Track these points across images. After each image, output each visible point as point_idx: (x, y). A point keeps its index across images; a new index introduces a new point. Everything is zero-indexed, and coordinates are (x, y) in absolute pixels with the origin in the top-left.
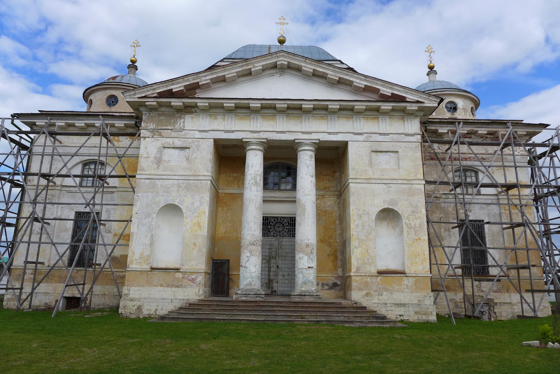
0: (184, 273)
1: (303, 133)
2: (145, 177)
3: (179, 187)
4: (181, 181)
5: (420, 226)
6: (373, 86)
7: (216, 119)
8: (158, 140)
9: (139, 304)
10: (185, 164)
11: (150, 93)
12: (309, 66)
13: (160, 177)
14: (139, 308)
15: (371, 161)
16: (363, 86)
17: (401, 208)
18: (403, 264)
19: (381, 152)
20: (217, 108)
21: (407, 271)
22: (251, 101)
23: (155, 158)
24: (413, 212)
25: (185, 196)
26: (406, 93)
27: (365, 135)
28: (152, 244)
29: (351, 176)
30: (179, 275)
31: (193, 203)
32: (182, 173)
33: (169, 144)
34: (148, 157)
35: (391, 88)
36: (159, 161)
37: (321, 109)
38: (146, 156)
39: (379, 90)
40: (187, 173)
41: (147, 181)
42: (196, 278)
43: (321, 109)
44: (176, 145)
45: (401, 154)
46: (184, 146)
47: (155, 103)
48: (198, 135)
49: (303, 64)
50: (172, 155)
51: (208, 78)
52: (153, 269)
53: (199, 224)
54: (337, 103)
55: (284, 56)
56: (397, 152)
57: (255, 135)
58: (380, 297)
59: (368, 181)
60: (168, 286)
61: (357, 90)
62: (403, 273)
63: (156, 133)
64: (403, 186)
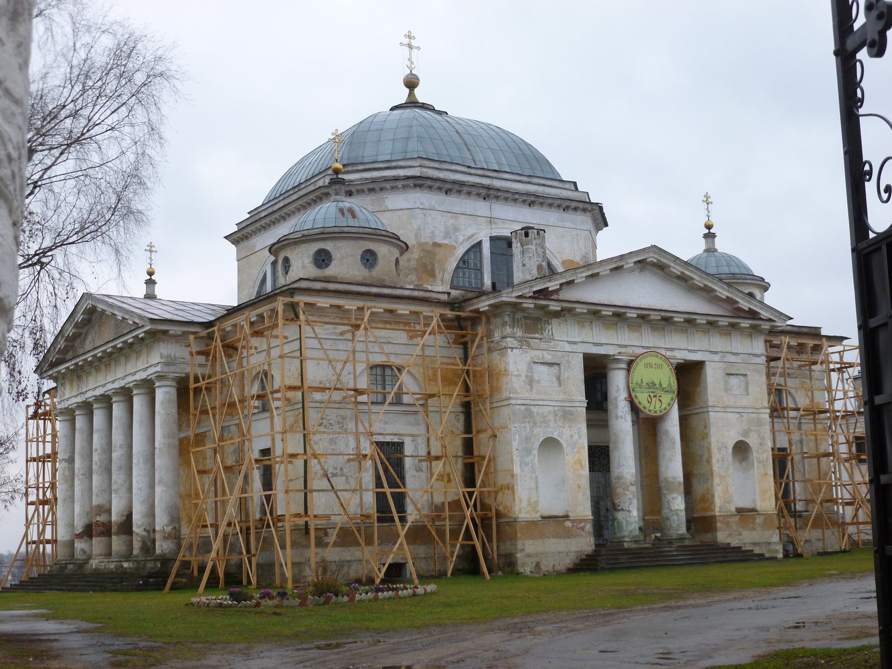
0: (573, 521)
2: (519, 402)
3: (556, 415)
4: (556, 408)
5: (767, 459)
6: (734, 298)
7: (583, 326)
8: (527, 352)
9: (537, 559)
10: (556, 384)
11: (526, 291)
12: (678, 267)
13: (536, 403)
14: (538, 565)
16: (724, 297)
18: (754, 501)
19: (732, 374)
20: (595, 314)
21: (758, 509)
22: (628, 310)
23: (526, 376)
24: (761, 444)
25: (563, 427)
26: (762, 309)
27: (721, 354)
28: (537, 488)
29: (710, 404)
31: (572, 436)
32: (556, 398)
33: (539, 358)
34: (519, 375)
36: (531, 381)
37: (690, 323)
38: (516, 373)
39: (737, 302)
40: (562, 397)
41: (523, 408)
42: (585, 526)
43: (690, 323)
44: (546, 360)
45: (750, 378)
46: (554, 361)
47: (532, 306)
48: (568, 348)
49: (672, 265)
50: (542, 372)
52: (543, 517)
54: (705, 317)
55: (654, 252)
56: (745, 375)
57: (623, 350)
58: (740, 537)
59: (725, 409)
61: (714, 299)
62: (754, 510)
63: (524, 343)
64: (753, 415)
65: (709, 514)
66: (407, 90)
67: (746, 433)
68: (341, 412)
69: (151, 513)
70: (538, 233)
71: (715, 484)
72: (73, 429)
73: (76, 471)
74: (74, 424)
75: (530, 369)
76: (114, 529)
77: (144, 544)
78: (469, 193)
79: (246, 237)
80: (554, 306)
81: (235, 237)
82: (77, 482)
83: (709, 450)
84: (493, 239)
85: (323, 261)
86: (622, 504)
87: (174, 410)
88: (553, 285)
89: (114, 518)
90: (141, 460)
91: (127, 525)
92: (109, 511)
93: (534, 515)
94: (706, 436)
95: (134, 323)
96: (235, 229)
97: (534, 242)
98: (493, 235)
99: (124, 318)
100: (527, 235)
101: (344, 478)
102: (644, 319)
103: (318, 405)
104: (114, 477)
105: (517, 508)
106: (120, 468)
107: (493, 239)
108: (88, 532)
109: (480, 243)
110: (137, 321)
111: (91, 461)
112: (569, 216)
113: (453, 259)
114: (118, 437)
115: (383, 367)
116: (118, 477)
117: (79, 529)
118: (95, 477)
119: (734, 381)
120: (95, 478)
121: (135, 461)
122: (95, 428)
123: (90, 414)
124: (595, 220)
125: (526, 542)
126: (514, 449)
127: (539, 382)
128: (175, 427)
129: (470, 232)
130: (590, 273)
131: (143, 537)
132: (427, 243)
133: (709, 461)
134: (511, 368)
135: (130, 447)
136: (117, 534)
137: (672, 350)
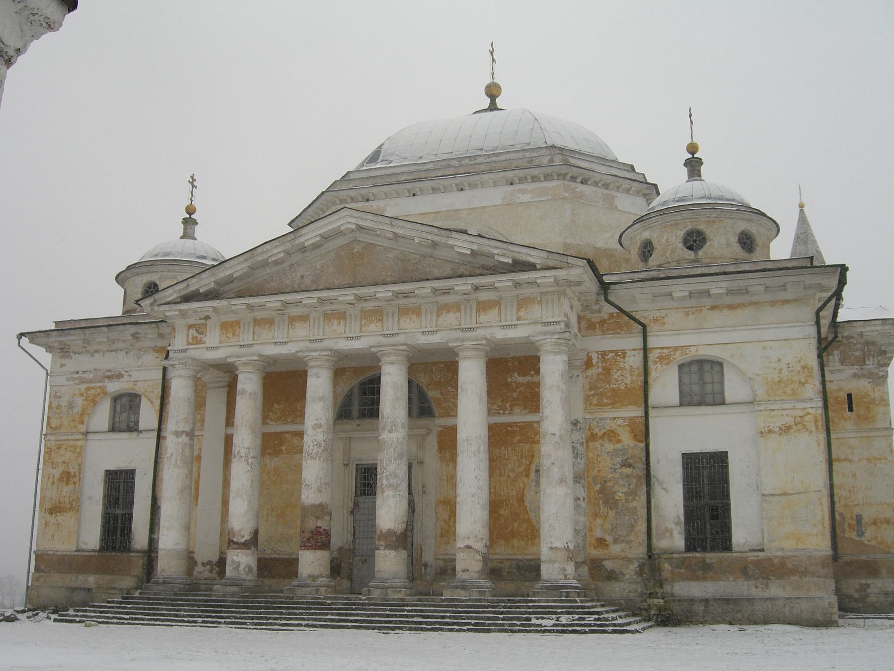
90: (482, 448)
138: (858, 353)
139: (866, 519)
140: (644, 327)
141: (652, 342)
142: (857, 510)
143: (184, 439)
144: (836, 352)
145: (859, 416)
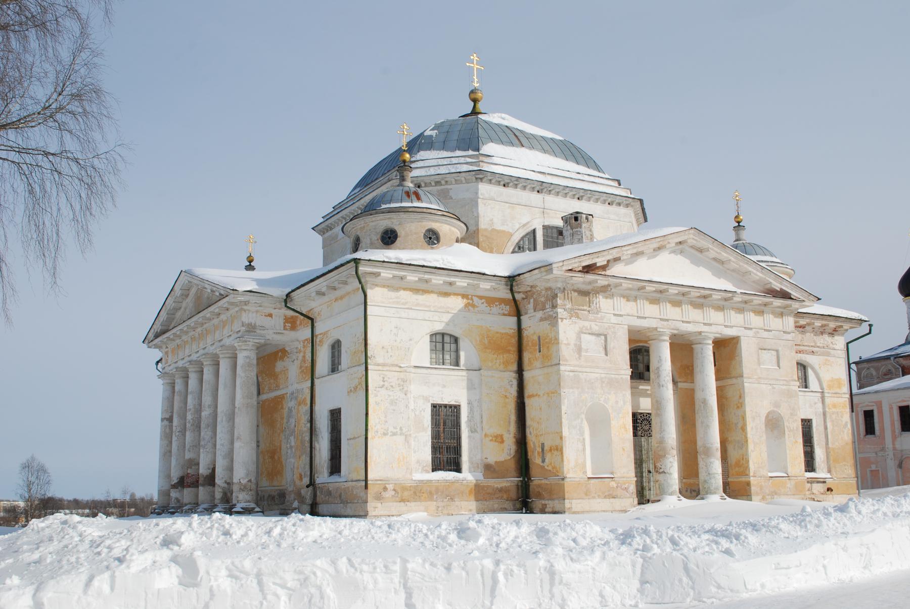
1: (705, 324)
3: (603, 382)
10: (603, 354)
11: (576, 265)
13: (584, 370)
15: (759, 359)
17: (784, 411)
23: (575, 345)
24: (791, 414)
30: (613, 484)
31: (617, 402)
35: (781, 283)
36: (579, 350)
37: (725, 302)
41: (571, 374)
48: (614, 320)
50: (589, 341)
51: (629, 252)
53: (625, 427)
57: (665, 323)
60: (605, 497)
63: (574, 314)
64: (784, 387)
65: (743, 479)
66: (472, 104)
67: (777, 405)
68: (402, 375)
69: (230, 469)
70: (587, 218)
71: (750, 450)
72: (174, 392)
73: (174, 428)
74: (174, 387)
75: (579, 338)
76: (201, 481)
77: (225, 494)
78: (524, 188)
79: (330, 228)
80: (602, 281)
81: (320, 227)
82: (174, 438)
83: (744, 418)
84: (545, 228)
85: (390, 238)
86: (663, 467)
87: (253, 374)
88: (600, 262)
89: (201, 471)
91: (211, 479)
92: (198, 464)
93: (581, 475)
94: (741, 405)
95: (221, 294)
96: (322, 220)
97: (584, 225)
98: (546, 224)
99: (212, 291)
100: (576, 219)
101: (403, 437)
102: (685, 296)
103: (380, 368)
104: (202, 434)
105: (565, 469)
106: (208, 426)
107: (545, 228)
108: (182, 483)
109: (534, 231)
110: (222, 292)
111: (185, 419)
112: (614, 208)
113: (510, 243)
114: (207, 399)
115: (443, 335)
116: (206, 434)
117: (175, 481)
118: (188, 433)
119: (765, 355)
120: (188, 434)
121: (219, 419)
122: (189, 390)
123: (186, 378)
124: (636, 215)
125: (574, 501)
126: (563, 413)
127: (587, 351)
128: (254, 390)
129: (524, 221)
130: (635, 251)
131: (223, 488)
132: (486, 230)
133: (744, 429)
134: (562, 336)
135: (217, 407)
136: (203, 485)
137: (710, 325)
138: (543, 299)
139: (546, 448)
140: (312, 320)
141: (318, 331)
142: (542, 440)
143: (166, 423)
144: (532, 300)
145: (543, 356)
